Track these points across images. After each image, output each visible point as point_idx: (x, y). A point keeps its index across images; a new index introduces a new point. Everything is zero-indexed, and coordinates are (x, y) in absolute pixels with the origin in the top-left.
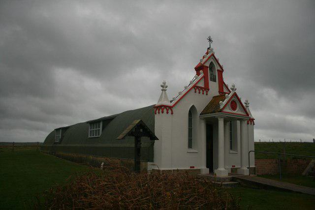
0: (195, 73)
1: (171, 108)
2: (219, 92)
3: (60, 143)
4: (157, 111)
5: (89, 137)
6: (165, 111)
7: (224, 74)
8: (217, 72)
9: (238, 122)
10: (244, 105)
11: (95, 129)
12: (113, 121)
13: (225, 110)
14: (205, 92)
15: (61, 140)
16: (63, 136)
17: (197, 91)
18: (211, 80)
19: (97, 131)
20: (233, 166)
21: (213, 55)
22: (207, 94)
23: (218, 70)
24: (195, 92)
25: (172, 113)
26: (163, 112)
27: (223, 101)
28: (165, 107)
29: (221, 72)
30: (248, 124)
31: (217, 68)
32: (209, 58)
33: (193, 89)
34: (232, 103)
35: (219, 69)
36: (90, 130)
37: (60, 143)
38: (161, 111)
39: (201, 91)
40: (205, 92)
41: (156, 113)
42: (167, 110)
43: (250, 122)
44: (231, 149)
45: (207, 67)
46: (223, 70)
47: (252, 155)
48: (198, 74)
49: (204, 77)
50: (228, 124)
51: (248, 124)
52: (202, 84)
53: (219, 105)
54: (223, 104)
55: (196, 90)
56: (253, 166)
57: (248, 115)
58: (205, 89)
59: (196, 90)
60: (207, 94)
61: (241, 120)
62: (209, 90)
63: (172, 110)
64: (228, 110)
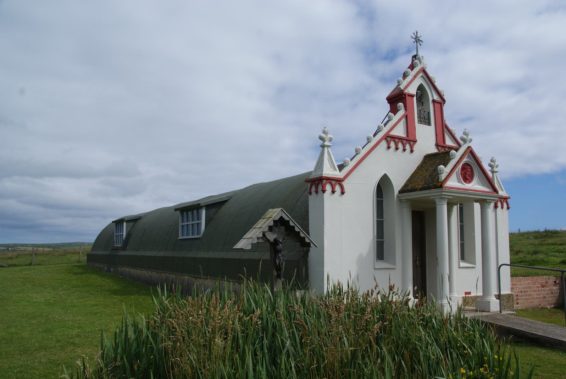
0: (388, 107)
1: (339, 181)
2: (437, 145)
3: (124, 248)
4: (313, 189)
5: (180, 237)
6: (328, 188)
7: (445, 108)
9: (477, 207)
10: (487, 169)
11: (191, 223)
12: (227, 204)
13: (450, 183)
14: (408, 147)
15: (126, 242)
16: (129, 235)
17: (392, 144)
18: (420, 122)
19: (196, 226)
20: (466, 293)
21: (424, 71)
22: (412, 151)
24: (389, 148)
25: (343, 193)
26: (324, 191)
27: (445, 165)
28: (330, 180)
29: (441, 102)
30: (496, 207)
31: (432, 96)
32: (415, 77)
34: (463, 168)
35: (436, 97)
36: (180, 224)
37: (124, 248)
38: (320, 188)
39: (400, 146)
40: (408, 147)
41: (310, 193)
43: (499, 204)
44: (462, 257)
45: (412, 96)
46: (444, 101)
47: (506, 272)
48: (394, 110)
50: (455, 209)
51: (496, 207)
52: (400, 131)
53: (436, 173)
54: (445, 170)
55: (389, 143)
56: (506, 291)
57: (496, 191)
60: (412, 151)
61: (483, 202)
62: (415, 141)
64: (453, 183)
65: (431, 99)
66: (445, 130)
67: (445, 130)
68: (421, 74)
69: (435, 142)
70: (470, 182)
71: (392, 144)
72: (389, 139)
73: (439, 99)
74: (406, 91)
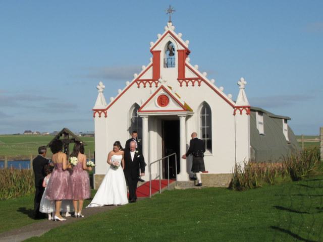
1: (103, 110)
8: (176, 53)
23: (178, 51)
24: (139, 87)
25: (106, 116)
30: (234, 114)
31: (177, 47)
33: (135, 84)
39: (148, 85)
40: (154, 84)
42: (100, 114)
43: (238, 112)
45: (160, 51)
49: (152, 65)
51: (234, 114)
55: (139, 84)
58: (153, 80)
59: (139, 84)
63: (106, 114)
65: (176, 49)
66: (186, 68)
67: (186, 68)
68: (169, 34)
69: (177, 78)
70: (166, 105)
71: (142, 85)
72: (139, 82)
73: (183, 48)
74: (154, 50)
